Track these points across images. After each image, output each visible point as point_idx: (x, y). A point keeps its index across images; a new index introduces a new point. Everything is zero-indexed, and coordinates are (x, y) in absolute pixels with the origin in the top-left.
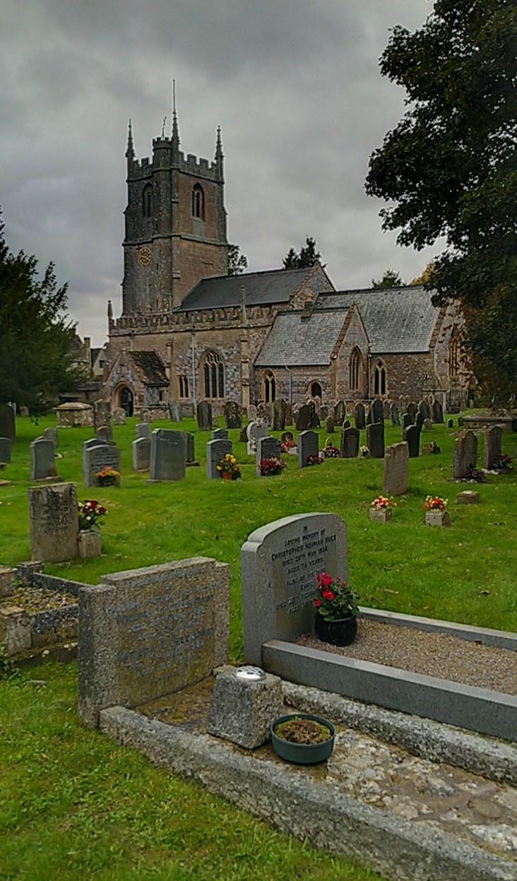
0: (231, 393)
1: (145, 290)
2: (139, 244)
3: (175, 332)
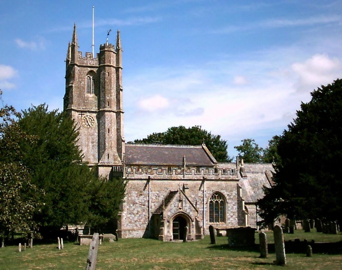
0: (231, 219)
1: (88, 146)
2: (82, 112)
3: (190, 180)
